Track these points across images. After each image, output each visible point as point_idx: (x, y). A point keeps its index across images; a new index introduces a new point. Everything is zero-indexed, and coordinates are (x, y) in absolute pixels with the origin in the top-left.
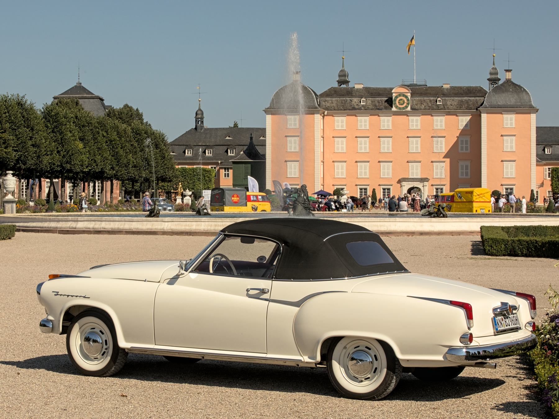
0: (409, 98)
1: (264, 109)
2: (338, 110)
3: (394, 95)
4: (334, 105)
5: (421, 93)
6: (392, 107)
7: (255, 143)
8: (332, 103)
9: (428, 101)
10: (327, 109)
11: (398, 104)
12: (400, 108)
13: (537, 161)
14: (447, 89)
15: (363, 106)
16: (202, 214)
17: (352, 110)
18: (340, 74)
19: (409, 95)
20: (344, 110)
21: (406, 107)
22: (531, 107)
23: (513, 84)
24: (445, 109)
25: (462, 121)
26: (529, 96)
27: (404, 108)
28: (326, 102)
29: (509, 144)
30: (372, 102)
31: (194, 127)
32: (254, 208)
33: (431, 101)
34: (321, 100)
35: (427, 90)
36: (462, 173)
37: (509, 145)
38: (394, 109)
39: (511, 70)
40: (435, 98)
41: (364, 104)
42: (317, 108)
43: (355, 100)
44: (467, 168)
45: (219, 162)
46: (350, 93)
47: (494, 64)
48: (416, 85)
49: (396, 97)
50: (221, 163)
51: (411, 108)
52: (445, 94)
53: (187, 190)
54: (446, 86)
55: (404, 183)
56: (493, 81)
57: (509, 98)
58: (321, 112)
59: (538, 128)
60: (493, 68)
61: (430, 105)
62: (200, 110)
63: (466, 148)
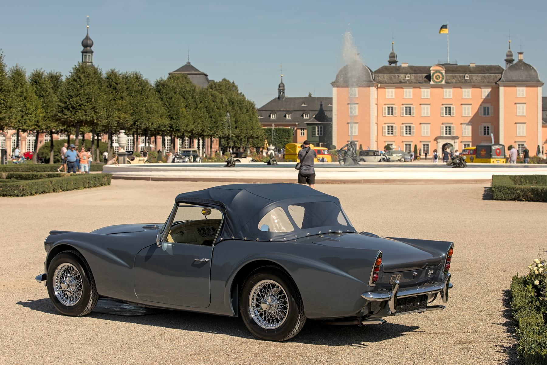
0: (444, 74)
1: (331, 82)
3: (432, 72)
4: (386, 79)
6: (430, 81)
7: (324, 109)
8: (384, 78)
9: (459, 76)
10: (380, 82)
11: (435, 79)
12: (436, 82)
13: (543, 123)
14: (473, 68)
15: (408, 80)
17: (399, 83)
19: (443, 72)
21: (442, 81)
22: (538, 81)
23: (524, 63)
24: (471, 83)
25: (485, 92)
26: (537, 73)
27: (439, 82)
29: (521, 110)
30: (415, 77)
31: (277, 96)
33: (460, 77)
35: (457, 68)
37: (521, 111)
38: (432, 83)
40: (464, 75)
42: (371, 82)
43: (402, 76)
45: (297, 124)
46: (398, 70)
47: (509, 48)
48: (449, 64)
49: (434, 74)
50: (298, 124)
51: (446, 82)
53: (271, 146)
54: (472, 65)
55: (439, 140)
56: (509, 61)
57: (522, 74)
58: (375, 85)
59: (543, 98)
60: (509, 52)
61: (460, 79)
62: (282, 83)
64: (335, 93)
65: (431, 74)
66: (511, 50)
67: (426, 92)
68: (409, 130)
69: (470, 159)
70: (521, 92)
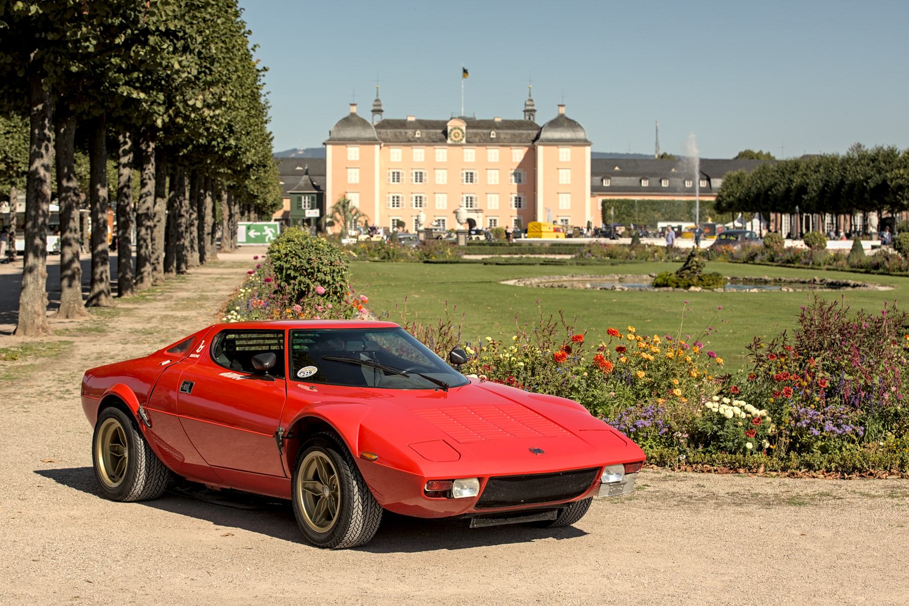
0: (464, 130)
4: (389, 137)
14: (499, 123)
15: (418, 138)
19: (464, 128)
21: (461, 140)
23: (567, 119)
33: (484, 134)
38: (449, 141)
43: (410, 132)
47: (530, 96)
49: (452, 130)
51: (467, 141)
65: (449, 131)
66: (532, 97)
67: (441, 153)
68: (419, 201)
70: (565, 153)
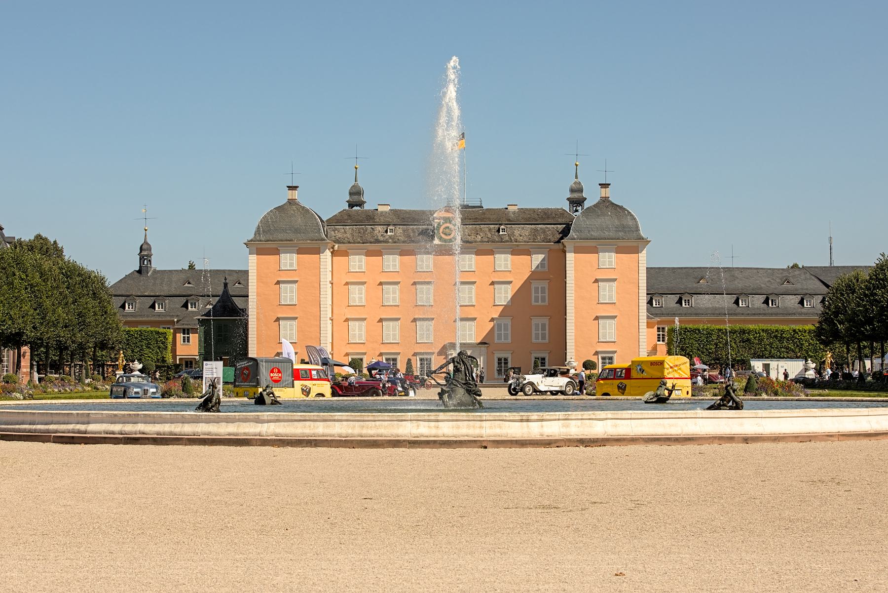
1: (246, 241)
2: (354, 243)
4: (348, 235)
5: (476, 218)
7: (231, 293)
8: (345, 233)
9: (487, 229)
10: (337, 241)
12: (445, 241)
13: (648, 317)
14: (514, 213)
15: (390, 237)
16: (267, 403)
17: (375, 243)
18: (352, 191)
20: (363, 243)
24: (511, 241)
28: (336, 232)
29: (608, 292)
30: (404, 231)
32: (305, 391)
33: (490, 230)
34: (329, 228)
35: (484, 214)
36: (537, 335)
39: (609, 184)
40: (497, 226)
41: (393, 234)
44: (543, 329)
45: (176, 320)
46: (371, 218)
52: (511, 219)
58: (330, 246)
59: (649, 270)
61: (489, 235)
62: (146, 242)
63: (543, 300)
64: (252, 263)
69: (619, 387)
